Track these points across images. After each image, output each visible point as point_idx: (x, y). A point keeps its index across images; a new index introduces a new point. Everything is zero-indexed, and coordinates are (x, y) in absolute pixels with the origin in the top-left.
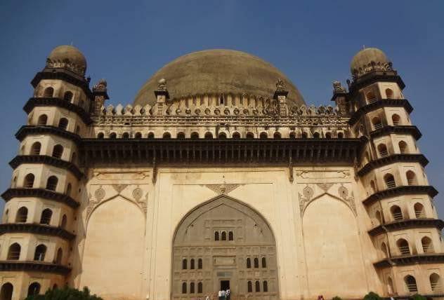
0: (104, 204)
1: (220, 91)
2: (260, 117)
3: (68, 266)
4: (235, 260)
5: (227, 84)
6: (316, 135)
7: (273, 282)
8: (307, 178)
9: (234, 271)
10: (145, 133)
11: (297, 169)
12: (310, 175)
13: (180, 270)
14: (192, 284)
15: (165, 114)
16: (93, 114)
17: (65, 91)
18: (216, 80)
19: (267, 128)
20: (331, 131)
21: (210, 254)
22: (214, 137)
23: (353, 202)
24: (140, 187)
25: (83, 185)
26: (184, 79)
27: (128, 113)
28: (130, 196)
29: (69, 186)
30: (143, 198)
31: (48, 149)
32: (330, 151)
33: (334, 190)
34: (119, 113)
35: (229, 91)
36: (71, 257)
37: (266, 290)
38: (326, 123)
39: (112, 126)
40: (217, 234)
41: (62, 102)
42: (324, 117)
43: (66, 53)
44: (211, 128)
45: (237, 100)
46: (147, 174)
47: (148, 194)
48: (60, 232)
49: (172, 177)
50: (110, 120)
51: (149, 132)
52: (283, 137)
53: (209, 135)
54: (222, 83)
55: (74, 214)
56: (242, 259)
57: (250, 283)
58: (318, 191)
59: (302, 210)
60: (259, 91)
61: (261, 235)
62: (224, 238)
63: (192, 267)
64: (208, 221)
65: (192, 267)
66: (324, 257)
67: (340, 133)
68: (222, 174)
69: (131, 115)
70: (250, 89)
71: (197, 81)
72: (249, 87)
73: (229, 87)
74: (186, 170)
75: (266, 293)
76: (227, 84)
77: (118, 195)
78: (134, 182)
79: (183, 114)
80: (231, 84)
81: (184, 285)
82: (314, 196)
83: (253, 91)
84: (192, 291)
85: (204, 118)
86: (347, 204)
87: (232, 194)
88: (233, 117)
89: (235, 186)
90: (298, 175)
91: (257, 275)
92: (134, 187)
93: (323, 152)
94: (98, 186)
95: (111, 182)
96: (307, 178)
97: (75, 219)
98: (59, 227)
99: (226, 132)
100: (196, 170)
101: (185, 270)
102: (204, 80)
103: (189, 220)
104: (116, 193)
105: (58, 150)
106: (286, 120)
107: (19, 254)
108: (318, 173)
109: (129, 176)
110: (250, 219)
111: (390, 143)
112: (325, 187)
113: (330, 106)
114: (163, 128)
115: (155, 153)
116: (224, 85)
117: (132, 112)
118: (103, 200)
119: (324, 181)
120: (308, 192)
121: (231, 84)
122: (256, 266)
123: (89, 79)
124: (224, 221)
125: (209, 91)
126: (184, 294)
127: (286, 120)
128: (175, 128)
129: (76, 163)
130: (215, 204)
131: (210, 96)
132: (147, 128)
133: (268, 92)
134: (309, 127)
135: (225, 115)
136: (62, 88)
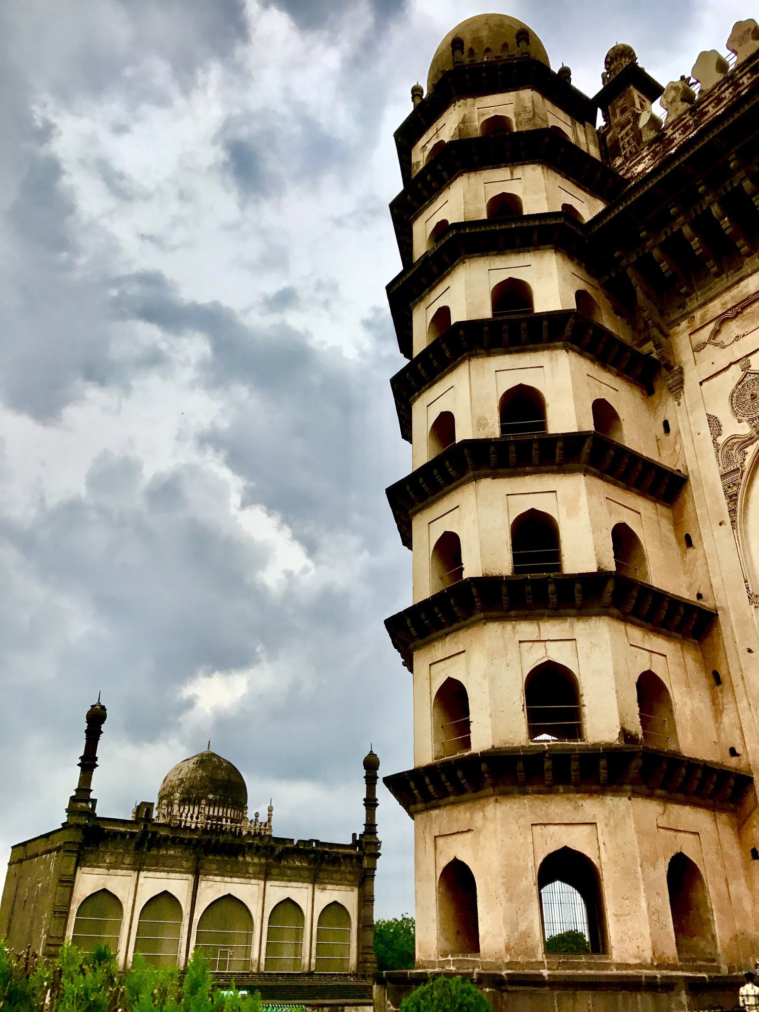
3: (732, 762)
25: (671, 403)
36: (727, 719)
48: (621, 594)
55: (677, 524)
94: (735, 368)
97: (689, 542)
107: (468, 723)
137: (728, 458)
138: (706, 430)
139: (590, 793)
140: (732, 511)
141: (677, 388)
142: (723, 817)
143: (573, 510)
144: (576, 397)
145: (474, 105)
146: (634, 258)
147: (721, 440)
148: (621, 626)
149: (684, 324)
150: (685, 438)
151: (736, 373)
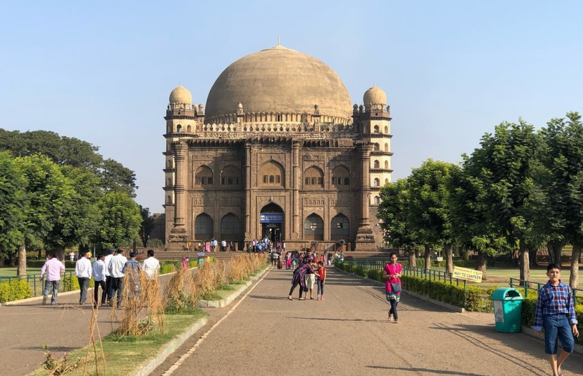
1: (278, 111)
15: (243, 130)
18: (275, 102)
27: (220, 130)
34: (214, 130)
38: (343, 137)
42: (342, 132)
54: (278, 105)
72: (298, 106)
73: (283, 107)
88: (286, 133)
116: (280, 106)
117: (223, 129)
125: (270, 111)
131: (271, 114)
133: (311, 107)
135: (280, 132)
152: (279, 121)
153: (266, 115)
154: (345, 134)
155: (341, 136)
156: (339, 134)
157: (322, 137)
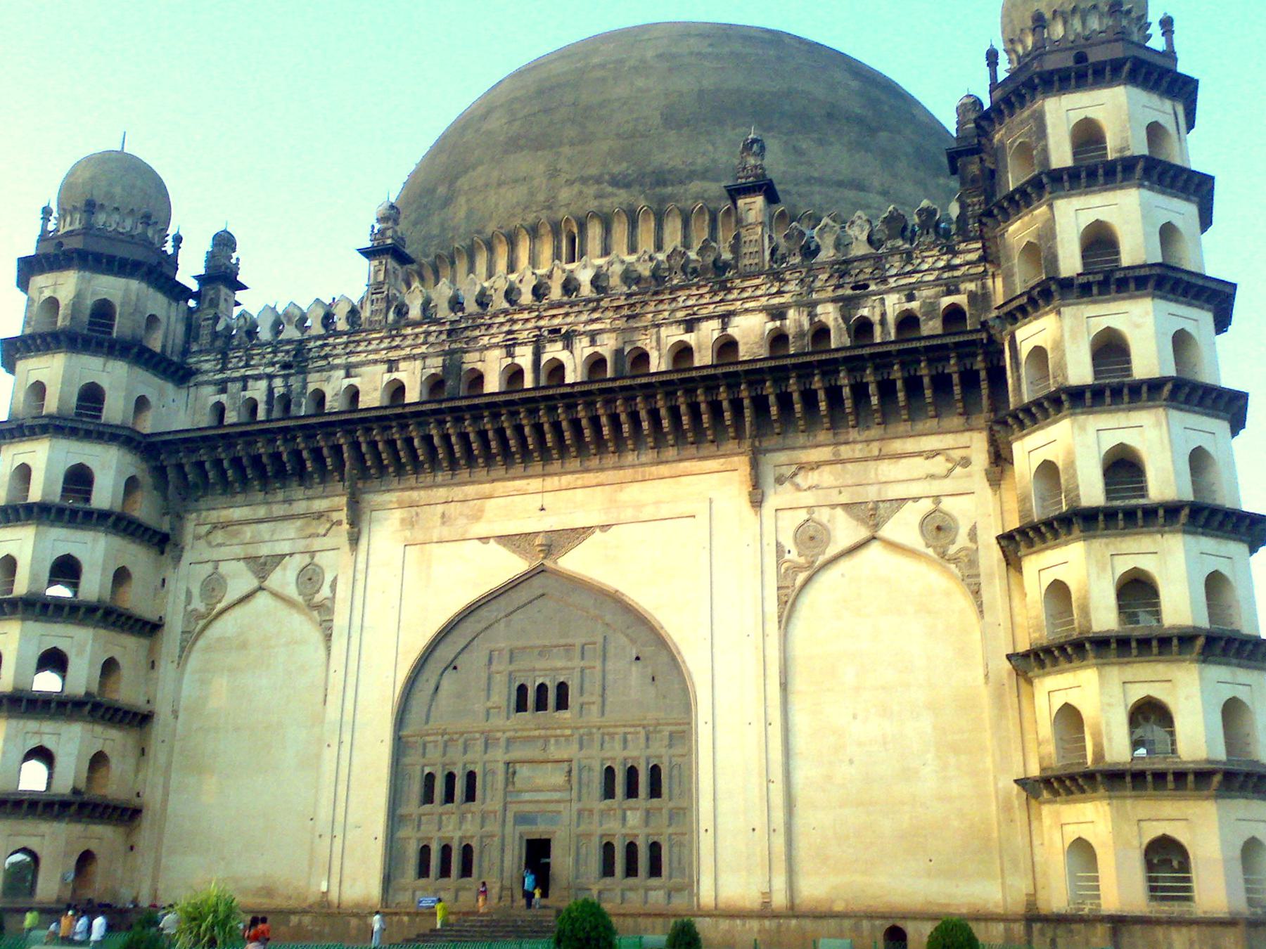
0: (226, 616)
1: (563, 214)
2: (673, 290)
3: (136, 801)
4: (570, 772)
5: (584, 180)
6: (863, 328)
7: (681, 845)
8: (809, 488)
9: (561, 807)
10: (334, 386)
11: (782, 457)
12: (825, 476)
13: (412, 806)
14: (446, 850)
16: (195, 348)
17: (89, 302)
18: (553, 173)
19: (690, 324)
20: (914, 305)
21: (499, 755)
22: (528, 382)
23: (973, 563)
24: (319, 559)
25: (171, 567)
26: (463, 183)
28: (292, 591)
29: (121, 576)
30: (325, 591)
31: (48, 480)
32: (887, 390)
33: (904, 526)
34: (264, 333)
35: (592, 205)
36: (140, 777)
37: (655, 870)
39: (245, 379)
40: (522, 690)
41: (93, 332)
42: (894, 251)
43: (93, 178)
44: (518, 350)
45: (620, 232)
46: (335, 516)
47: (335, 579)
49: (403, 520)
50: (241, 360)
51: (347, 382)
52: (744, 353)
53: (515, 374)
54: (570, 183)
55: (151, 650)
56: (590, 769)
57: (608, 849)
58: (845, 531)
59: (788, 605)
60: (695, 186)
61: (652, 691)
62: (541, 705)
63: (449, 797)
64: (500, 651)
65: (449, 797)
66: (851, 762)
67: (953, 304)
68: (537, 500)
69: (297, 335)
70: (664, 183)
71: (499, 185)
72: (661, 178)
73: (591, 190)
74: (442, 493)
75: (654, 882)
76: (584, 180)
77: (261, 588)
78: (301, 545)
79: (444, 312)
80: (598, 180)
81: (425, 851)
82: (831, 551)
83: (680, 189)
84: (445, 872)
85: (501, 319)
86: (952, 575)
87: (572, 562)
88: (589, 301)
89: (577, 535)
90: (780, 480)
91: (631, 821)
92: (298, 562)
93: (860, 392)
95: (239, 551)
96: (809, 488)
97: (153, 665)
98: (88, 694)
99: (564, 356)
100: (471, 490)
101: (428, 806)
102: (516, 181)
103: (446, 652)
104: (255, 583)
105: (79, 479)
106: (757, 287)
108: (849, 466)
109: (290, 530)
110: (623, 640)
111: (1059, 345)
112: (872, 515)
113: (925, 203)
114: (385, 367)
115: (346, 455)
116: (576, 187)
118: (220, 606)
119: (871, 494)
120: (811, 536)
121: (598, 180)
122: (632, 792)
123: (178, 240)
124: (543, 652)
125: (531, 218)
126: (423, 881)
127: (757, 287)
128: (419, 363)
129: (144, 509)
130: (522, 595)
131: (534, 232)
132: (342, 373)
134: (834, 300)
136: (79, 296)
137: (189, 622)
138: (183, 597)
139: (45, 820)
140: (180, 657)
141: (178, 559)
142: (121, 830)
143: (80, 653)
144: (104, 570)
145: (89, 281)
146: (173, 461)
147: (190, 608)
148: (89, 727)
149: (194, 515)
150: (171, 598)
151: (208, 568)
152: (572, 259)
153: (512, 242)
154: (909, 257)
155: (893, 271)
156: (878, 262)
157: (780, 293)
